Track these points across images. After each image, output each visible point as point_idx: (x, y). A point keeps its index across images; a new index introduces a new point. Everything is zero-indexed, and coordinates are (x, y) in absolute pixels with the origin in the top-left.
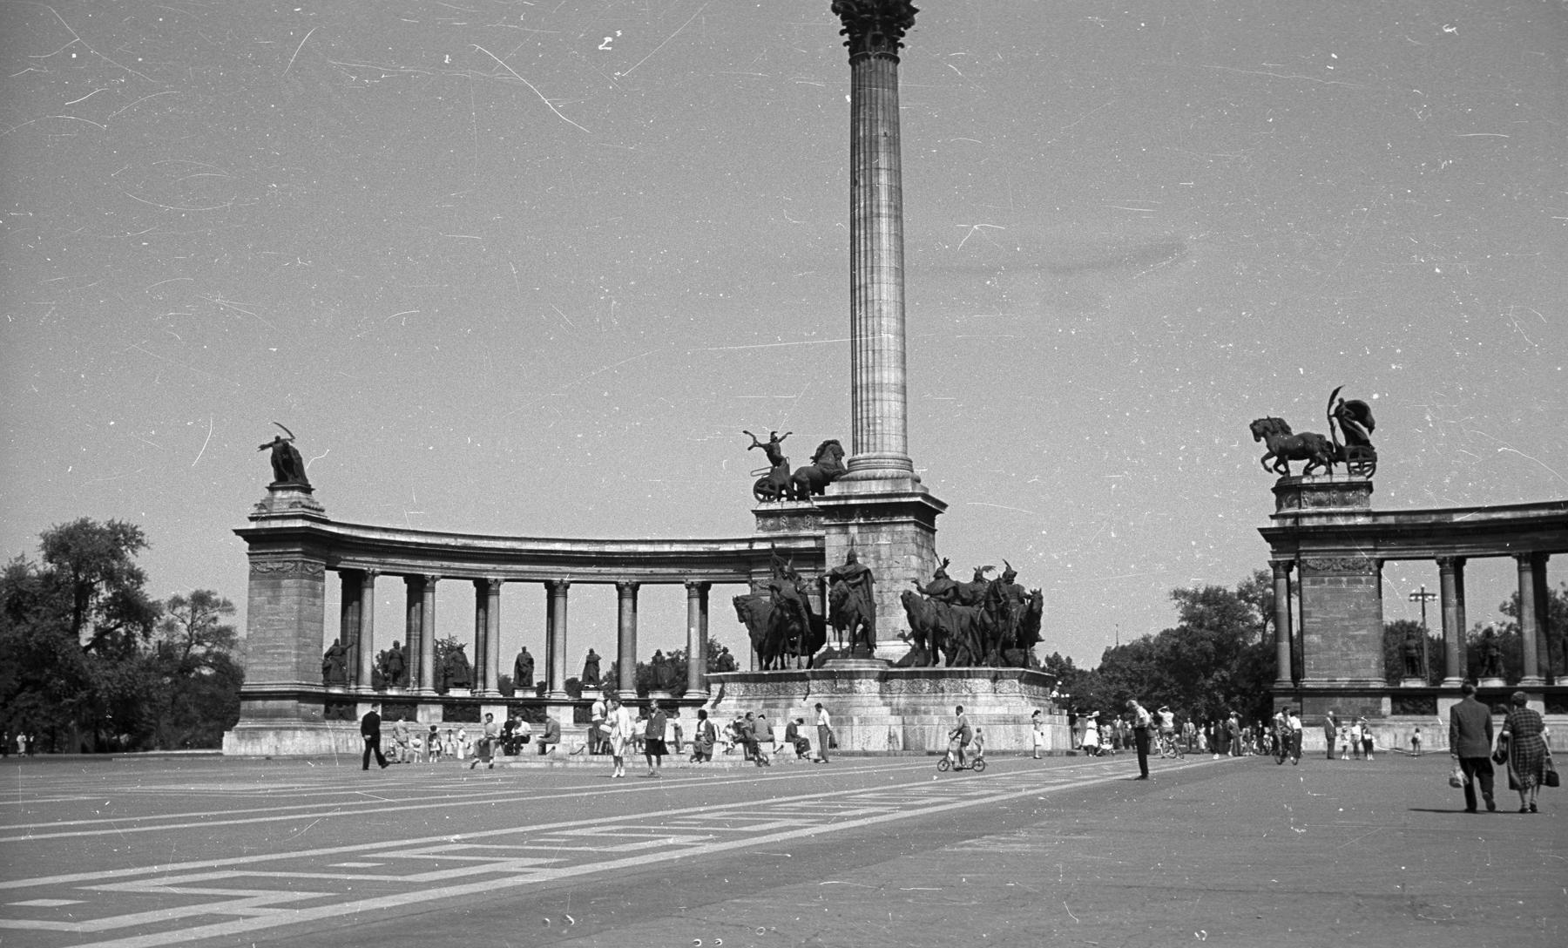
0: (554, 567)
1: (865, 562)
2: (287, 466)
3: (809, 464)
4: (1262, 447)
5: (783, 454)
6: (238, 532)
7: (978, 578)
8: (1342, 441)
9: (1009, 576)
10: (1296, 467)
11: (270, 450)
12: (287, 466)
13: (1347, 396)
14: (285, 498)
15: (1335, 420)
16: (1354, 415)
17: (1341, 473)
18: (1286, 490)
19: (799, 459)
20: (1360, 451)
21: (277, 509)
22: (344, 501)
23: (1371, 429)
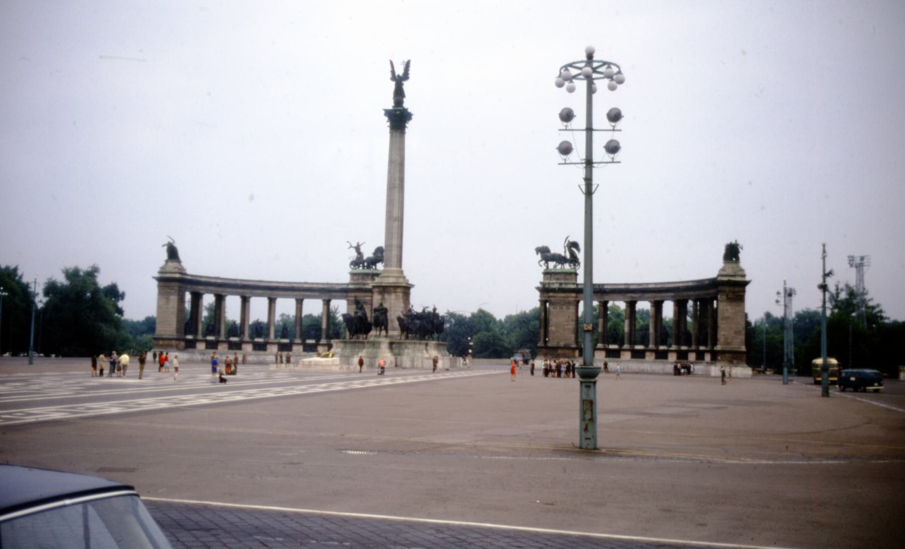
0: (272, 291)
1: (386, 305)
2: (173, 253)
4: (539, 257)
6: (154, 278)
7: (424, 311)
8: (568, 256)
9: (435, 310)
10: (552, 264)
11: (166, 247)
12: (173, 253)
13: (571, 239)
14: (172, 265)
17: (567, 267)
18: (547, 273)
19: (368, 253)
21: (168, 269)
22: (194, 265)
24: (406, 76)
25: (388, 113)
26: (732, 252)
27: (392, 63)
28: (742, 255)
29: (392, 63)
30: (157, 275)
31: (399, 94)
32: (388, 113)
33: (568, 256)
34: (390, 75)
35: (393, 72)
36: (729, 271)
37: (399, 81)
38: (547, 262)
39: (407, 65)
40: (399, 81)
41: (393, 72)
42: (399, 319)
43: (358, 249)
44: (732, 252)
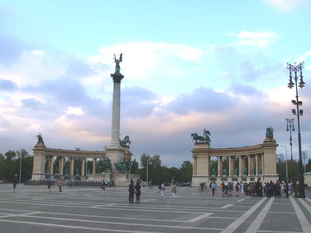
3: (123, 139)
4: (192, 138)
8: (205, 137)
10: (198, 141)
12: (40, 139)
13: (206, 130)
19: (122, 138)
22: (48, 144)
23: (210, 135)
25: (112, 75)
28: (274, 134)
30: (34, 148)
32: (112, 75)
33: (205, 137)
37: (118, 62)
38: (196, 141)
39: (121, 55)
40: (118, 62)
42: (116, 164)
44: (270, 132)
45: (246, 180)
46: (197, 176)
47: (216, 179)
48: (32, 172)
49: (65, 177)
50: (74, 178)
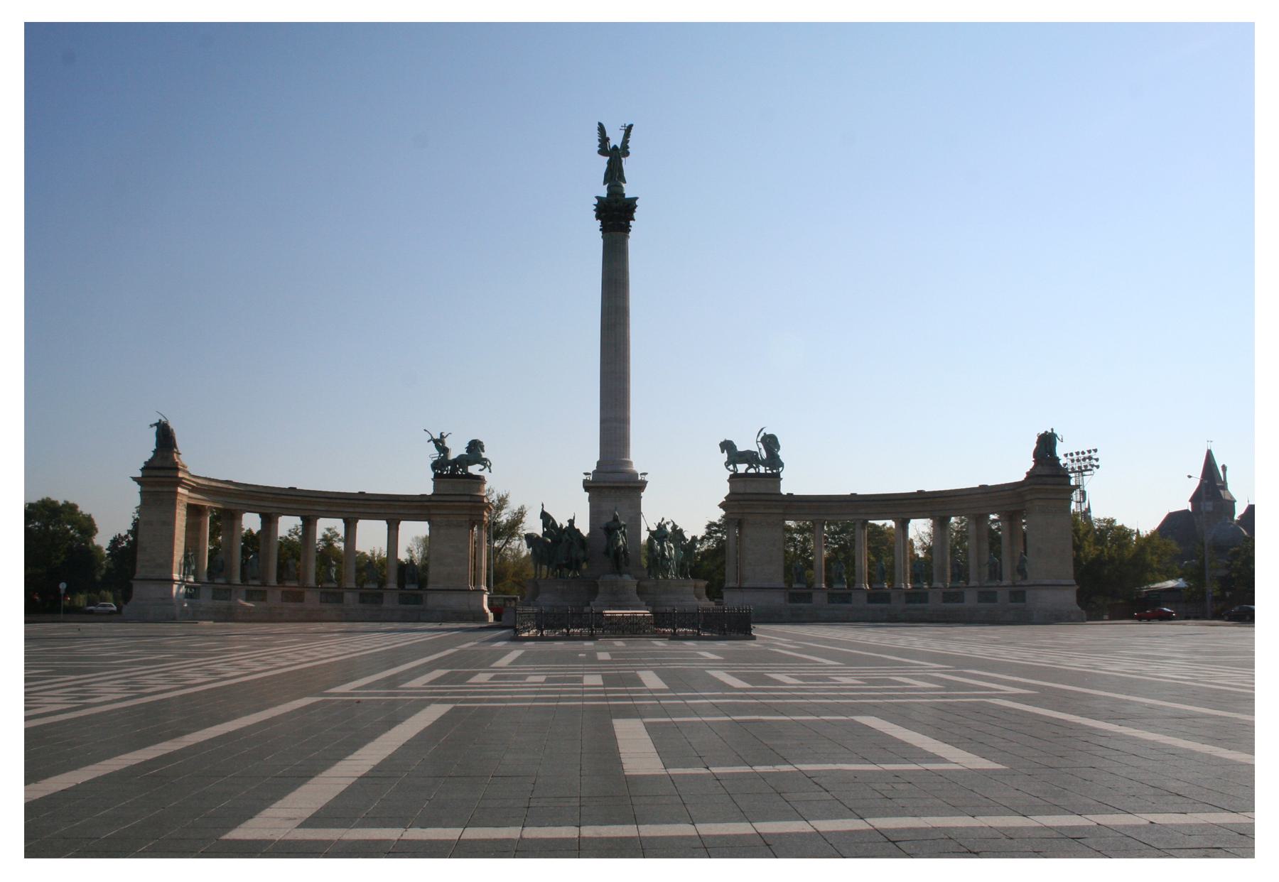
2: (165, 437)
3: (464, 452)
4: (725, 456)
5: (447, 445)
6: (135, 479)
10: (742, 468)
12: (165, 437)
15: (761, 445)
16: (770, 442)
19: (457, 449)
20: (774, 461)
24: (624, 150)
26: (1046, 443)
27: (601, 129)
28: (1060, 450)
29: (601, 129)
30: (139, 474)
31: (614, 175)
34: (596, 144)
35: (604, 139)
36: (1046, 471)
37: (615, 157)
40: (615, 157)
41: (604, 139)
43: (439, 443)
44: (1046, 443)
45: (926, 602)
46: (746, 585)
47: (810, 594)
48: (134, 572)
49: (248, 591)
50: (278, 593)
